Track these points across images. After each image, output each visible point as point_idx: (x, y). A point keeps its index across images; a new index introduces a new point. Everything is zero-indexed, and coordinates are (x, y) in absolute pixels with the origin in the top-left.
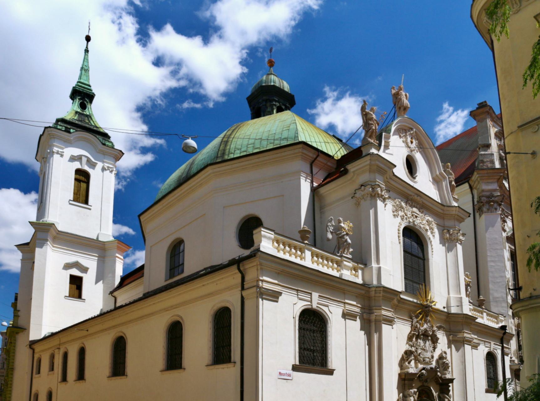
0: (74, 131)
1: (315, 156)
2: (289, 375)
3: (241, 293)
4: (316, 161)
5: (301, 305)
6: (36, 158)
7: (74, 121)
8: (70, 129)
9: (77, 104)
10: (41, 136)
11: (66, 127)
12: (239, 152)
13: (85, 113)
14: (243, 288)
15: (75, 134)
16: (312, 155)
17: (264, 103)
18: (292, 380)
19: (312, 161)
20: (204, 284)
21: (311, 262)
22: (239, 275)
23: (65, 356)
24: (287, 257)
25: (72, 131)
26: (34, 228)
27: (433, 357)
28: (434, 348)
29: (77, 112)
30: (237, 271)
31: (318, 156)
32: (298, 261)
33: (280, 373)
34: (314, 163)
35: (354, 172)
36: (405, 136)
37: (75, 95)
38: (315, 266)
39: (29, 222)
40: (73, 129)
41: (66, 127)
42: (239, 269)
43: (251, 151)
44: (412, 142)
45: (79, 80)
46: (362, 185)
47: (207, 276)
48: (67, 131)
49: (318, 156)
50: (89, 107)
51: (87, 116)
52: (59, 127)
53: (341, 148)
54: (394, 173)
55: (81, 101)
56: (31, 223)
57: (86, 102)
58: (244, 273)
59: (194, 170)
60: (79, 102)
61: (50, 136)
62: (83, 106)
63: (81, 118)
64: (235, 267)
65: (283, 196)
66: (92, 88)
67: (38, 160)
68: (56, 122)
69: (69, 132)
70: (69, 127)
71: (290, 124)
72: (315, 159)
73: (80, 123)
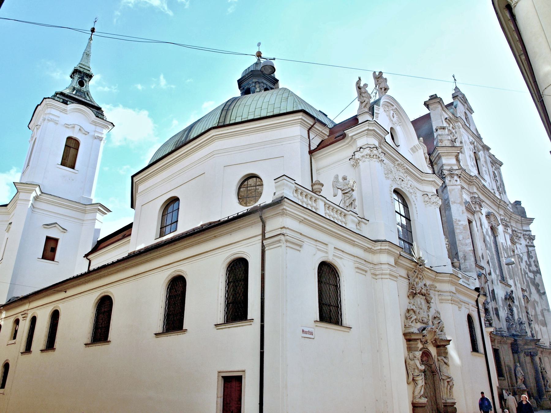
0: (71, 103)
3: (263, 243)
8: (67, 101)
14: (264, 238)
17: (254, 84)
25: (68, 103)
27: (428, 316)
28: (429, 308)
40: (70, 102)
41: (63, 100)
42: (261, 217)
46: (361, 148)
50: (87, 84)
51: (84, 93)
60: (79, 80)
61: (47, 106)
62: (81, 84)
69: (67, 104)
70: (67, 99)
73: (77, 97)
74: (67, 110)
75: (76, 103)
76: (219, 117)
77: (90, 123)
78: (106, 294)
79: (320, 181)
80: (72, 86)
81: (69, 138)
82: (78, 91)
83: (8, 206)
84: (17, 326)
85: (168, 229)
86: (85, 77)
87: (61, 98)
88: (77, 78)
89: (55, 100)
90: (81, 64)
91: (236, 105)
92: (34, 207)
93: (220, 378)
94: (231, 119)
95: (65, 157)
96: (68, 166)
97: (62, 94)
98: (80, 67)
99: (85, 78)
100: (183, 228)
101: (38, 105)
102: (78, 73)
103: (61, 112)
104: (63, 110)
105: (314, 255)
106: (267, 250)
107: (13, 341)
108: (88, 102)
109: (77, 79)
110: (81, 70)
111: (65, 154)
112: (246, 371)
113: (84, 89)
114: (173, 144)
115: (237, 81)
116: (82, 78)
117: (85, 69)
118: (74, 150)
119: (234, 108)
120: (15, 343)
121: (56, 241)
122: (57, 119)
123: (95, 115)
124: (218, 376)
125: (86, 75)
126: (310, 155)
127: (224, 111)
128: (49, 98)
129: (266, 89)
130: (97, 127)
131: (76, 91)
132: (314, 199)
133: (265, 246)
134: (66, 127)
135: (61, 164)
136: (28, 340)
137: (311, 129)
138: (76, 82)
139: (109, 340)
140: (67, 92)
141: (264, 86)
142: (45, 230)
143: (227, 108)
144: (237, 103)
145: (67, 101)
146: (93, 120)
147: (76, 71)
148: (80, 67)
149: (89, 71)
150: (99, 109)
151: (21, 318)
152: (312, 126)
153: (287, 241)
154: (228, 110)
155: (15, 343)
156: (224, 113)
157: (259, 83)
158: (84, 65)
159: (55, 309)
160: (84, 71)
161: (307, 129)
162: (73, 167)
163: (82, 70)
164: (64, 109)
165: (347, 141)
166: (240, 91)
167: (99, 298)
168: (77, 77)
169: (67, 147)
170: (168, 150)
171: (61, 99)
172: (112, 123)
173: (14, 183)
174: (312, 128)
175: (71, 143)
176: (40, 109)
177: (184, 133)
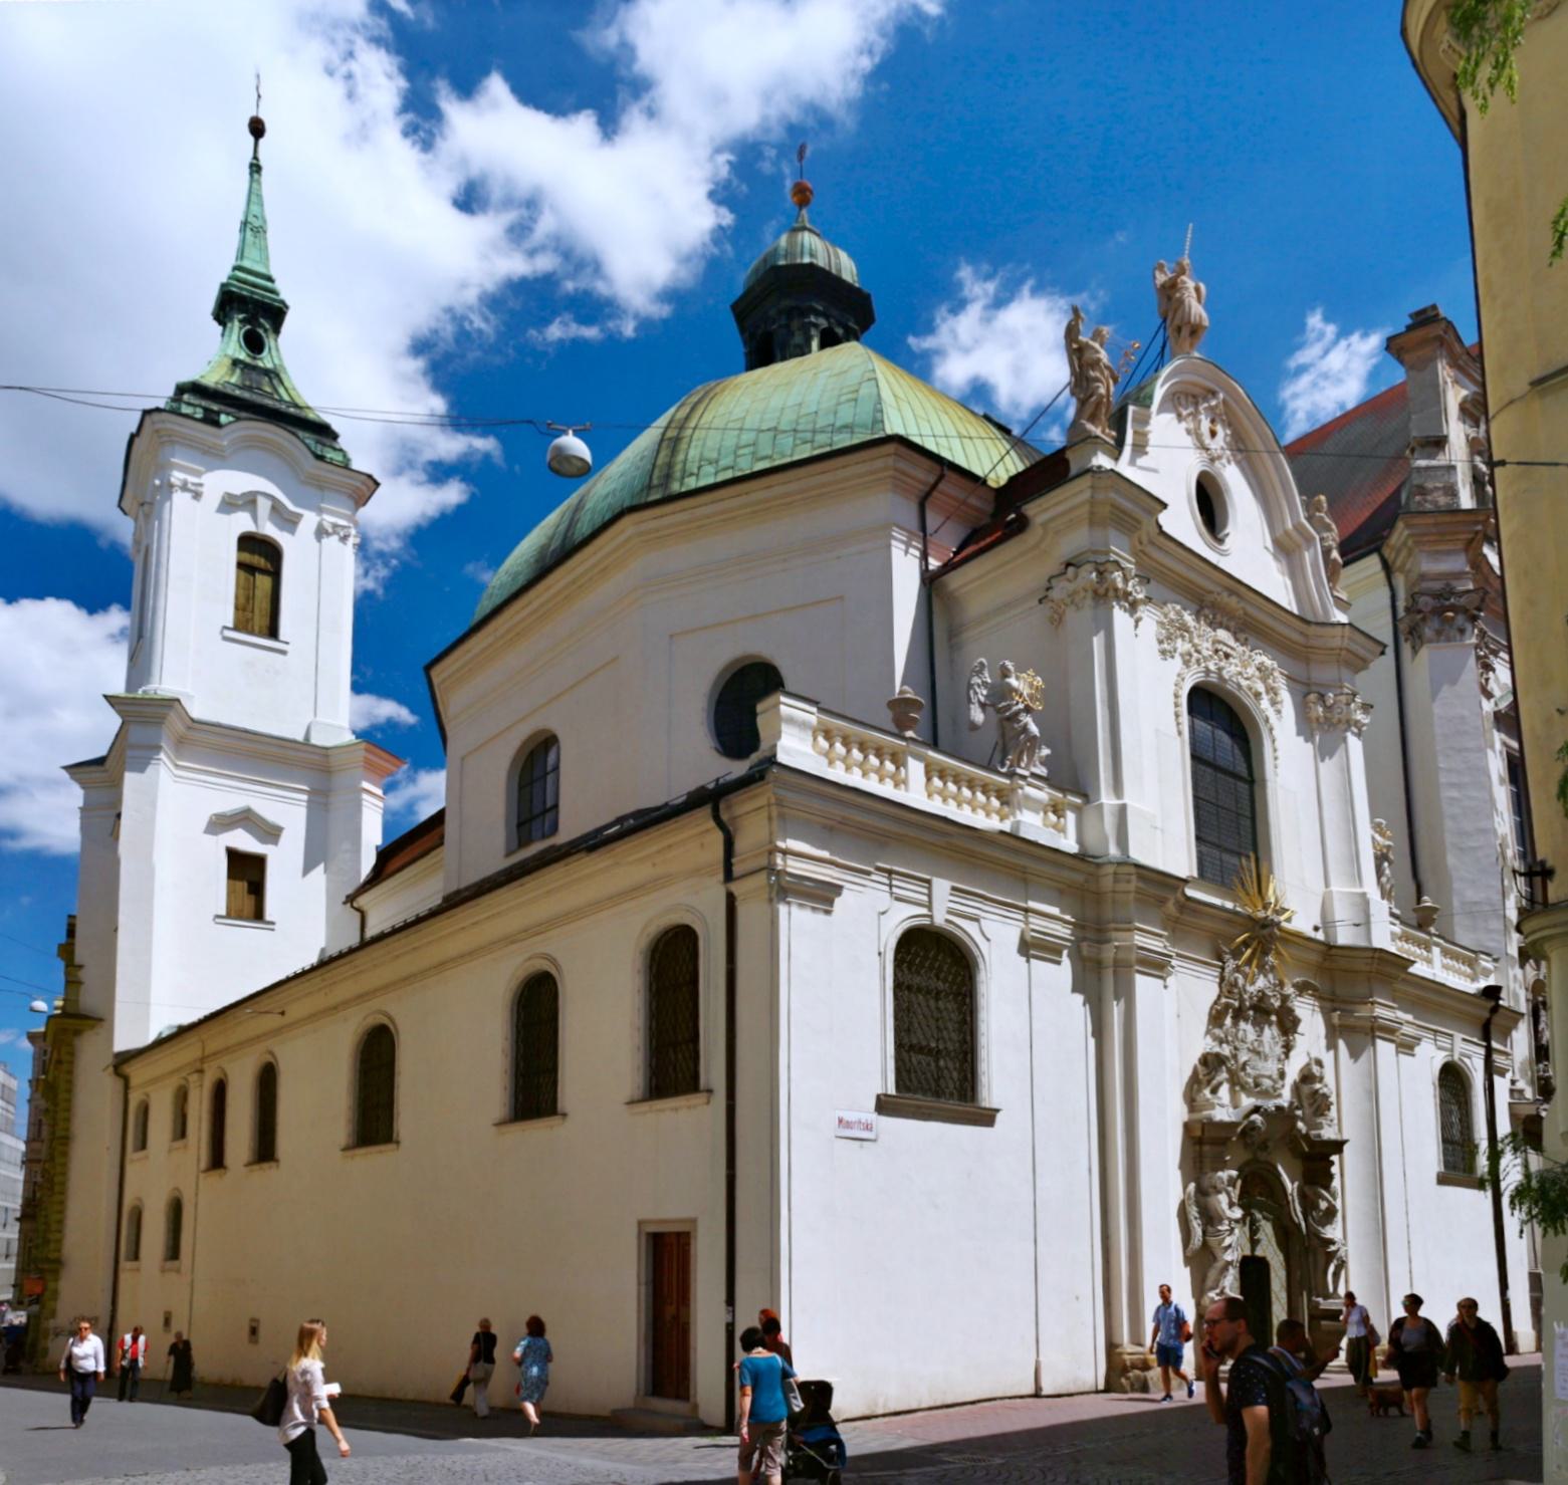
0: (231, 419)
1: (932, 479)
2: (868, 1127)
4: (935, 493)
5: (901, 918)
6: (119, 506)
7: (229, 390)
8: (218, 413)
9: (235, 337)
10: (132, 438)
11: (206, 410)
12: (711, 469)
13: (260, 364)
14: (729, 876)
15: (235, 428)
16: (924, 474)
18: (875, 1141)
19: (922, 494)
21: (926, 794)
22: (718, 837)
23: (220, 1092)
24: (855, 779)
25: (223, 419)
26: (119, 712)
29: (236, 363)
30: (712, 824)
31: (941, 477)
32: (886, 790)
33: (840, 1121)
34: (931, 499)
35: (1044, 525)
36: (1195, 415)
37: (228, 308)
38: (935, 806)
39: (106, 697)
40: (228, 414)
41: (206, 410)
43: (746, 466)
44: (1213, 434)
45: (239, 263)
47: (626, 839)
48: (211, 419)
49: (941, 477)
51: (267, 372)
52: (185, 409)
53: (1008, 452)
54: (1160, 527)
55: (248, 327)
56: (111, 700)
57: (261, 331)
58: (731, 828)
59: (584, 528)
60: (243, 331)
61: (160, 437)
62: (254, 343)
63: (250, 380)
64: (707, 810)
65: (841, 598)
66: (278, 285)
67: (126, 510)
68: (176, 394)
69: (217, 424)
70: (215, 407)
71: (860, 384)
72: (934, 487)
73: (246, 395)
87: (200, 406)
99: (262, 321)
100: (572, 824)
140: (211, 380)
165: (1029, 538)
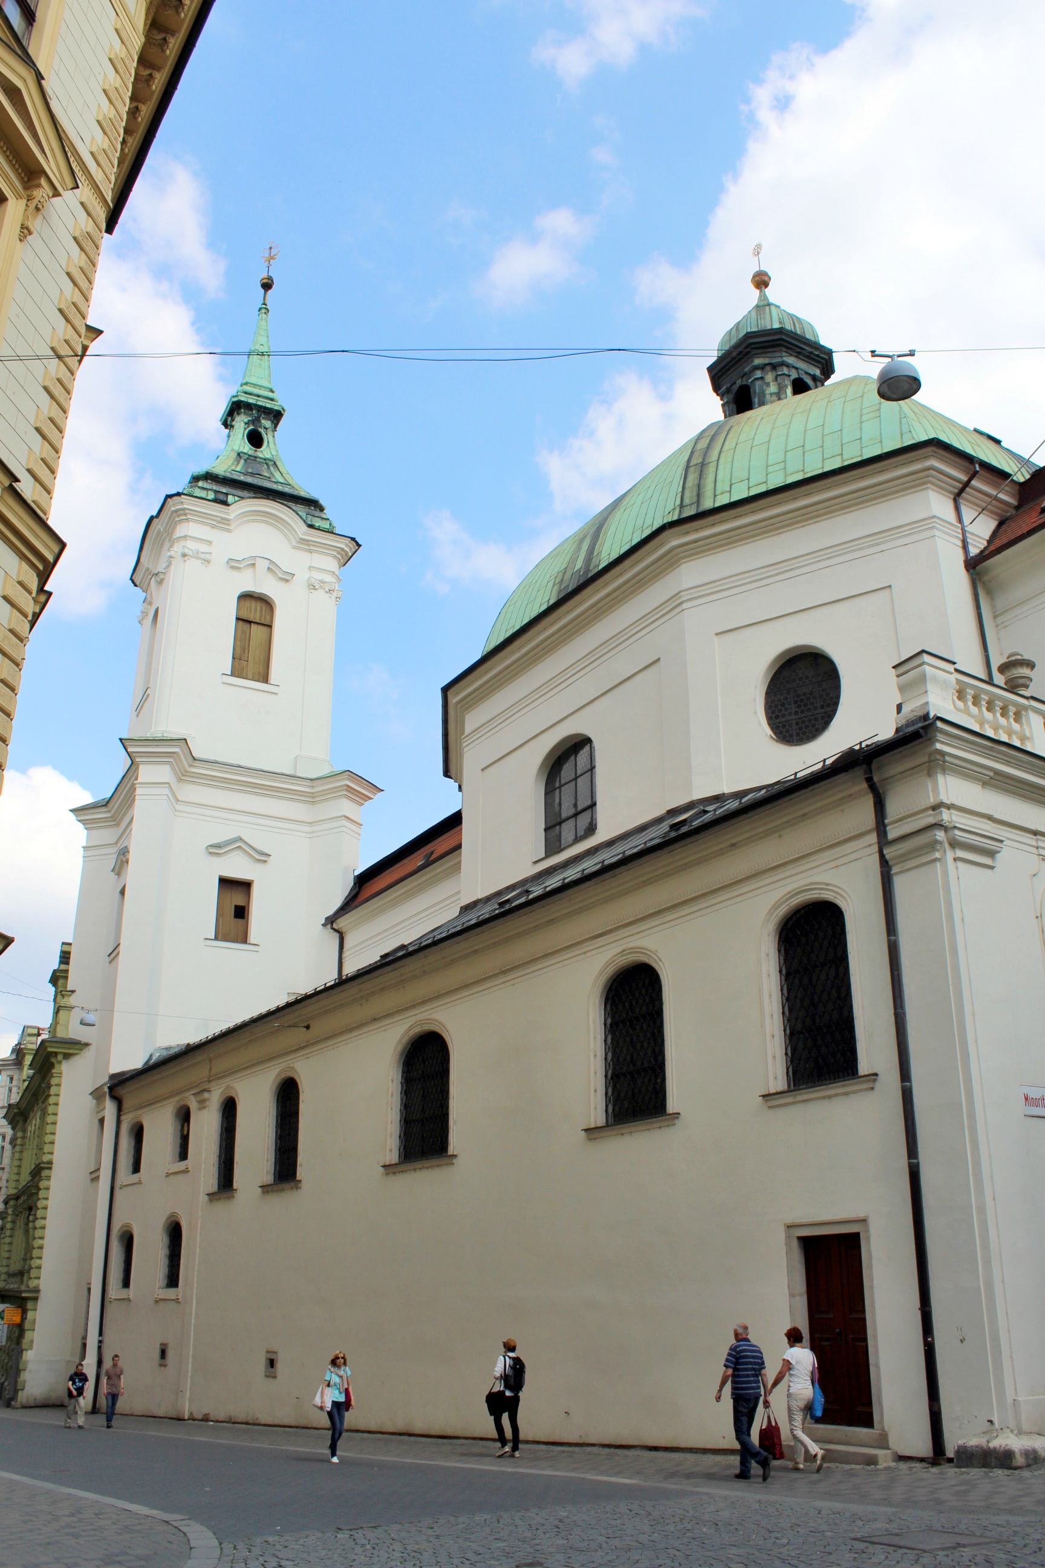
0: (237, 498)
3: (882, 856)
7: (235, 477)
8: (227, 494)
13: (260, 455)
15: (242, 506)
20: (734, 841)
22: (869, 802)
25: (230, 499)
29: (239, 455)
30: (865, 785)
41: (216, 492)
42: (869, 780)
47: (750, 814)
55: (252, 427)
57: (262, 431)
58: (881, 791)
59: (610, 549)
62: (256, 440)
63: (252, 468)
64: (859, 773)
67: (138, 584)
69: (225, 503)
70: (224, 490)
73: (249, 480)
74: (228, 520)
75: (250, 498)
76: (680, 489)
77: (294, 548)
78: (428, 1027)
79: (1021, 653)
80: (232, 450)
81: (246, 597)
82: (251, 459)
83: (110, 805)
84: (186, 1124)
85: (567, 832)
86: (263, 418)
87: (211, 490)
88: (243, 425)
89: (196, 497)
90: (246, 384)
91: (726, 448)
92: (178, 800)
93: (795, 1244)
94: (718, 492)
95: (238, 651)
96: (250, 675)
97: (209, 477)
98: (246, 393)
99: (263, 421)
101: (152, 519)
102: (242, 410)
103: (213, 527)
104: (219, 522)
105: (1034, 875)
106: (897, 874)
107: (182, 1165)
108: (280, 488)
109: (243, 430)
110: (251, 401)
111: (238, 643)
112: (870, 1221)
113: (264, 452)
114: (551, 584)
115: (706, 371)
116: (256, 421)
117: (259, 396)
118: (260, 628)
119: (723, 455)
120: (186, 1171)
121: (245, 886)
122: (204, 548)
123: (305, 521)
124: (788, 1237)
125: (265, 413)
126: (971, 571)
127: (691, 470)
128: (178, 494)
129: (800, 387)
130: (315, 555)
131: (245, 460)
132: (1012, 709)
133: (890, 863)
134: (233, 568)
135: (233, 674)
136: (220, 1160)
137: (963, 495)
138: (240, 436)
139: (451, 1151)
141: (790, 374)
142: (215, 859)
143: (700, 460)
144: (727, 443)
145: (227, 494)
146: (301, 536)
147: (236, 408)
148: (246, 393)
149: (272, 400)
150: (312, 504)
151: (193, 1105)
152: (967, 484)
153: (954, 844)
154: (703, 465)
155: (186, 1171)
156: (692, 478)
157: (774, 367)
158: (255, 385)
159: (283, 1076)
160: (260, 403)
161: (952, 497)
162: (265, 679)
163: (251, 400)
164: (222, 519)
166: (718, 398)
167: (405, 1039)
168: (241, 423)
169: (241, 623)
170: (539, 600)
171: (210, 492)
172: (353, 539)
173: (121, 740)
174: (967, 489)
175: (251, 611)
176: (159, 526)
177: (579, 548)
